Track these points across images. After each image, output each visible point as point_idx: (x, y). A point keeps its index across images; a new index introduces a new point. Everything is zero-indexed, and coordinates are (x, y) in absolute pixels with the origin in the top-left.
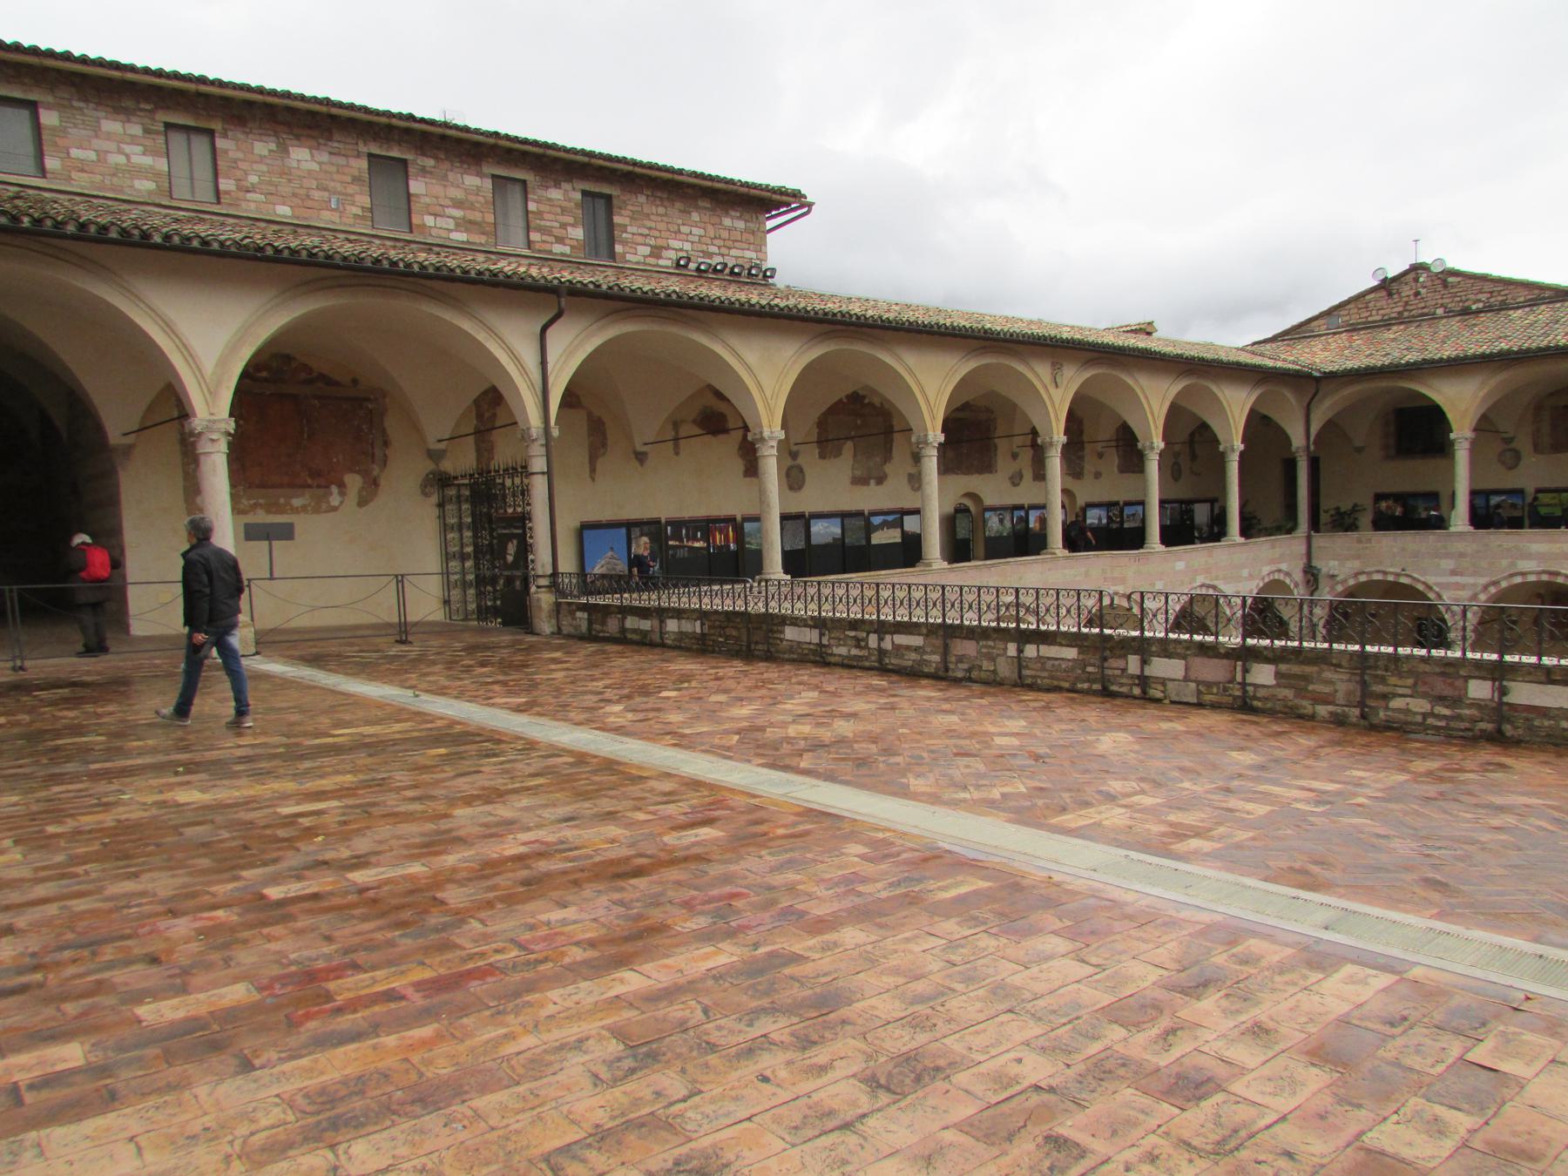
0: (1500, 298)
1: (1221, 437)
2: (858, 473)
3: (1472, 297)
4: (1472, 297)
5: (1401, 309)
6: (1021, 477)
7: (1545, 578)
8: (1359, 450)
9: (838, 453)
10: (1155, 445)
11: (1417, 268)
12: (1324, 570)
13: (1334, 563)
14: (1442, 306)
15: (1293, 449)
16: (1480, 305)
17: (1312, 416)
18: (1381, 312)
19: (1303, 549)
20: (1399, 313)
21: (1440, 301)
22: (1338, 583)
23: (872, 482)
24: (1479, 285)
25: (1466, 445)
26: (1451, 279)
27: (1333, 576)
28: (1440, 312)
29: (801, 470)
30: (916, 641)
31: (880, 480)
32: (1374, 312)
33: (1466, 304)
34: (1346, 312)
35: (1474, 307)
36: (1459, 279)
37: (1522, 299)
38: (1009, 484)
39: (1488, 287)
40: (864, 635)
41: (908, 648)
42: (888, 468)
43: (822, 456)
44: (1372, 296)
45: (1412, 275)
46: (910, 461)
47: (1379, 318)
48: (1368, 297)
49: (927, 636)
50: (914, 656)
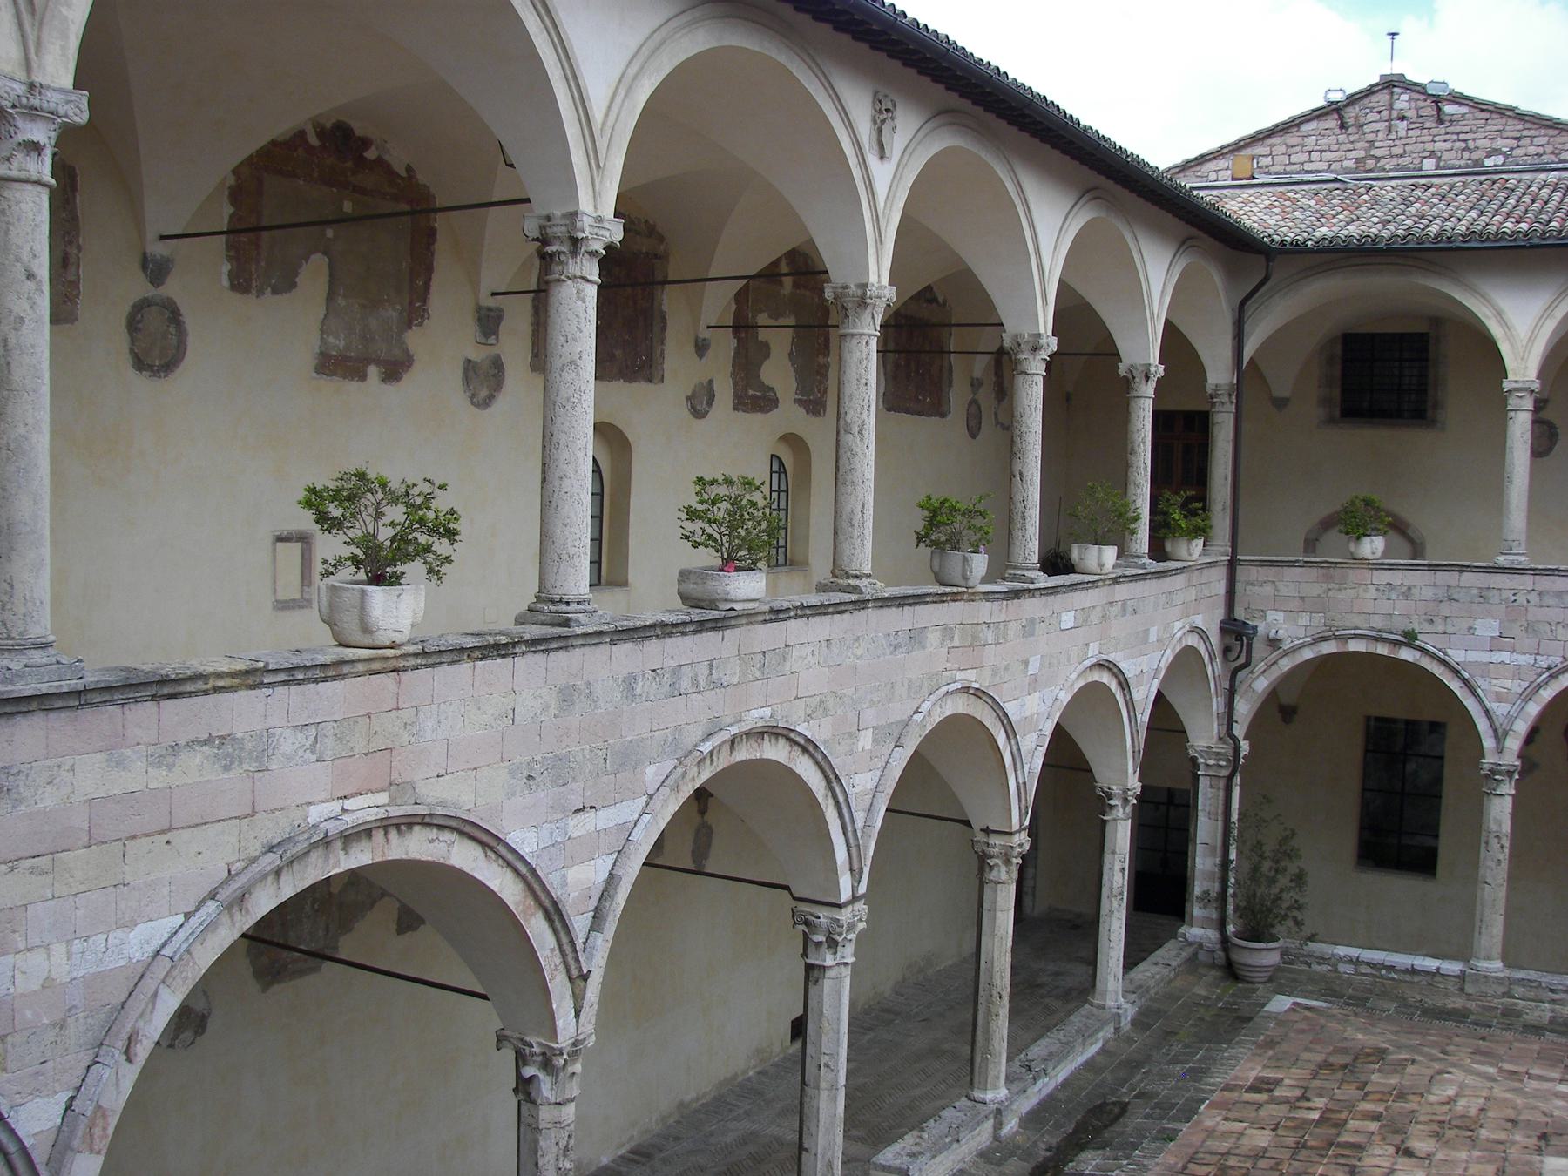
0: (1532, 150)
1: (1122, 346)
2: (338, 343)
5: (1362, 154)
6: (711, 398)
8: (1280, 403)
9: (286, 284)
10: (1043, 341)
11: (1391, 84)
12: (1261, 630)
13: (1272, 616)
15: (1209, 390)
16: (1500, 160)
17: (1247, 327)
18: (1328, 156)
19: (1220, 588)
21: (1429, 147)
22: (1286, 654)
23: (373, 371)
26: (1449, 109)
27: (1274, 643)
29: (174, 315)
31: (394, 370)
32: (1315, 155)
33: (1475, 156)
34: (1266, 150)
35: (1489, 162)
36: (1464, 110)
38: (685, 412)
39: (1513, 128)
42: (415, 340)
43: (241, 283)
44: (1313, 125)
45: (1382, 98)
46: (471, 329)
47: (1324, 166)
48: (1306, 128)
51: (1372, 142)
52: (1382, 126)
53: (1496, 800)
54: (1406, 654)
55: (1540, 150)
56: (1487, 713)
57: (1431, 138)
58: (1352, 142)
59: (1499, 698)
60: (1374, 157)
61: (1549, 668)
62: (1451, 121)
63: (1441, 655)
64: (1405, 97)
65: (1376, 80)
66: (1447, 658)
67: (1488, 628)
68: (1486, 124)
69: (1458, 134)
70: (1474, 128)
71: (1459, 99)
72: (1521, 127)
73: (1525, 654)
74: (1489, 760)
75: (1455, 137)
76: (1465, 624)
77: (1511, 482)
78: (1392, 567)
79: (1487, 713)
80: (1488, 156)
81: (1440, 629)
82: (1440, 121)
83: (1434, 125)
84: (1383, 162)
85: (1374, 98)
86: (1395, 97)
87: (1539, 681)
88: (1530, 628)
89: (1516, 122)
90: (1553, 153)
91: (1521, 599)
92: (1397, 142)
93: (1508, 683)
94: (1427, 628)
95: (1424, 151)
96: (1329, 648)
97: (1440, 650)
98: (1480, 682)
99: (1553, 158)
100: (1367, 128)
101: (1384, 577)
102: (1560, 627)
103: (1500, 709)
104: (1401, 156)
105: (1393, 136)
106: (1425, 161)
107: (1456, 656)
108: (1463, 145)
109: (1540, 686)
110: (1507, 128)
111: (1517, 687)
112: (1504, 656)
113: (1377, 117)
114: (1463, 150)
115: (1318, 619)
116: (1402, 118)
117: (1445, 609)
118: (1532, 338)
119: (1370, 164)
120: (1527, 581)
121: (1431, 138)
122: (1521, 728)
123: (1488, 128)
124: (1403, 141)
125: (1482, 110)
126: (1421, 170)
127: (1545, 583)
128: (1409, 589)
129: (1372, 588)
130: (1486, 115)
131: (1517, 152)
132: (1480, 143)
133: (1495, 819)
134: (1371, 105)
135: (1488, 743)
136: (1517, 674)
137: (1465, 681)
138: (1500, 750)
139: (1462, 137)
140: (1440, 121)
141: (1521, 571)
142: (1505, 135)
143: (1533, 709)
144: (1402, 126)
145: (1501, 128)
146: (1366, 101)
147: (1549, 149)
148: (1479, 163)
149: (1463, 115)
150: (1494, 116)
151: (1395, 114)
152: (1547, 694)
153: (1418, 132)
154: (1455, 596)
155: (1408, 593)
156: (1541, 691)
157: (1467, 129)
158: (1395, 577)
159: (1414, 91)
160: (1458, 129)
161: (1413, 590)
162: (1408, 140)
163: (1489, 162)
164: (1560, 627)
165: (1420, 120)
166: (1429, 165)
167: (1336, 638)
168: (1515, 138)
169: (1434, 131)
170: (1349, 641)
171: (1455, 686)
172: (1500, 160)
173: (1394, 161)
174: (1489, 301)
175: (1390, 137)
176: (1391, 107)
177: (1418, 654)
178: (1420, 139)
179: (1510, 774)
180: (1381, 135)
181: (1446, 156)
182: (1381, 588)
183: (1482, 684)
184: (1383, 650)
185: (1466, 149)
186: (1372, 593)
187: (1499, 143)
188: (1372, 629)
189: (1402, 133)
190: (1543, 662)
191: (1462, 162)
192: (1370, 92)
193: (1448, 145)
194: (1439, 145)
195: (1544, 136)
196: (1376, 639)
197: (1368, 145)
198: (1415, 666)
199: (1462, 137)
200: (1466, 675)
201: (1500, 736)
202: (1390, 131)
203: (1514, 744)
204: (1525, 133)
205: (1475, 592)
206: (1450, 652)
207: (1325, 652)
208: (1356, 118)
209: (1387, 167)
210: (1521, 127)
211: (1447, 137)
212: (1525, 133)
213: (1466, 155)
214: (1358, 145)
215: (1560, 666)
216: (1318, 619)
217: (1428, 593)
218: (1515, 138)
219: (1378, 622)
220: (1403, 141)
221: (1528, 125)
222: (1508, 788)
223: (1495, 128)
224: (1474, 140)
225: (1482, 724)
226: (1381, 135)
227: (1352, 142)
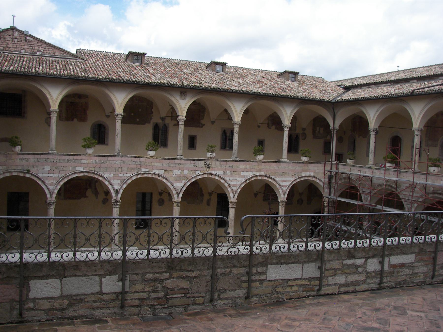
0: (48, 52)
3: (37, 48)
4: (37, 48)
5: (5, 46)
7: (86, 174)
11: (13, 29)
14: (24, 49)
16: (41, 53)
20: (3, 47)
21: (23, 47)
24: (40, 44)
25: (56, 115)
26: (28, 38)
28: (23, 52)
30: (409, 258)
33: (35, 51)
35: (38, 53)
36: (32, 39)
37: (57, 54)
39: (44, 46)
40: (363, 260)
41: (403, 266)
45: (11, 32)
49: (417, 254)
50: (407, 271)
51: (8, 43)
52: (11, 39)
53: (51, 210)
54: (28, 175)
55: (50, 52)
56: (48, 189)
57: (23, 45)
58: (2, 42)
59: (51, 185)
60: (8, 47)
61: (62, 177)
62: (28, 41)
63: (36, 175)
64: (17, 33)
65: (9, 27)
66: (38, 176)
67: (47, 168)
68: (37, 43)
69: (30, 45)
70: (34, 44)
71: (31, 36)
72: (46, 46)
73: (56, 174)
74: (49, 200)
75: (30, 45)
76: (43, 167)
77: (52, 133)
78: (23, 154)
79: (48, 189)
80: (38, 52)
81: (36, 169)
82: (26, 41)
83: (24, 41)
84: (11, 49)
85: (8, 32)
86: (14, 32)
87: (60, 180)
88: (57, 168)
89: (44, 44)
90: (53, 53)
91: (55, 161)
92: (15, 44)
93: (53, 181)
94: (33, 169)
95: (22, 48)
96: (8, 175)
97: (36, 174)
98: (46, 181)
99: (53, 54)
100: (6, 39)
101: (22, 156)
102: (64, 168)
103: (51, 188)
104: (16, 48)
105: (14, 42)
106: (22, 50)
107: (40, 175)
108: (32, 48)
109: (60, 181)
110: (38, 43)
111: (55, 182)
112: (52, 175)
113: (9, 37)
114: (32, 49)
115: (4, 168)
116: (16, 38)
117: (37, 164)
118: (57, 99)
119: (7, 49)
120: (57, 157)
121: (23, 45)
122: (56, 191)
123: (38, 45)
124: (16, 44)
125: (36, 40)
126: (21, 52)
127: (60, 157)
128: (28, 159)
129: (18, 159)
130: (38, 41)
131: (45, 52)
132: (36, 48)
133: (51, 214)
134: (7, 33)
135: (48, 196)
136: (55, 179)
137: (42, 181)
138: (51, 197)
139: (31, 46)
140: (26, 41)
141: (53, 154)
142: (42, 47)
143: (59, 187)
144: (16, 40)
145: (41, 45)
146: (6, 32)
147: (52, 52)
148: (35, 53)
149: (32, 40)
150: (39, 42)
151: (14, 37)
152: (62, 183)
153: (20, 43)
154: (40, 161)
155: (27, 160)
156: (60, 183)
157: (33, 44)
158: (24, 156)
159: (19, 32)
160: (30, 43)
161: (29, 160)
162: (17, 44)
163: (38, 53)
164: (64, 168)
165: (21, 40)
166: (23, 52)
167: (9, 172)
168: (44, 48)
169: (24, 43)
170: (13, 173)
171: (40, 183)
172: (41, 53)
173: (14, 49)
174: (47, 90)
175: (13, 43)
176: (13, 35)
177: (31, 175)
178: (21, 44)
179: (54, 203)
180: (10, 42)
181: (27, 50)
182: (21, 159)
183: (47, 182)
184: (21, 175)
185: (32, 49)
186: (18, 160)
187: (41, 49)
188: (19, 169)
189: (16, 42)
190: (61, 176)
191: (31, 52)
192: (7, 30)
193: (28, 47)
194: (26, 47)
195: (51, 49)
196: (20, 172)
197: (6, 44)
198: (29, 179)
199: (31, 46)
200: (43, 180)
201: (51, 194)
202: (13, 41)
203: (54, 196)
204: (47, 47)
205: (44, 159)
206: (38, 174)
207: (6, 176)
208: (3, 36)
209: (12, 50)
210: (46, 46)
211: (28, 45)
212: (47, 47)
213: (32, 50)
214: (4, 43)
215: (64, 177)
216: (4, 168)
217: (32, 160)
218: (44, 48)
219: (20, 168)
220: (16, 44)
221: (47, 45)
222: (53, 207)
223: (40, 45)
224: (34, 47)
225: (47, 191)
226: (10, 42)
227: (2, 42)
